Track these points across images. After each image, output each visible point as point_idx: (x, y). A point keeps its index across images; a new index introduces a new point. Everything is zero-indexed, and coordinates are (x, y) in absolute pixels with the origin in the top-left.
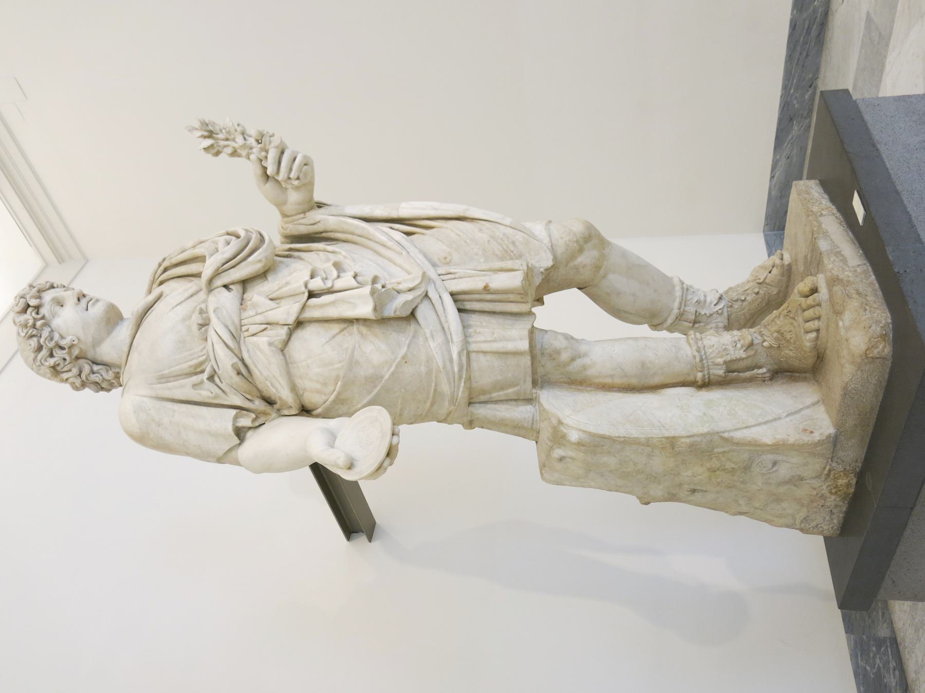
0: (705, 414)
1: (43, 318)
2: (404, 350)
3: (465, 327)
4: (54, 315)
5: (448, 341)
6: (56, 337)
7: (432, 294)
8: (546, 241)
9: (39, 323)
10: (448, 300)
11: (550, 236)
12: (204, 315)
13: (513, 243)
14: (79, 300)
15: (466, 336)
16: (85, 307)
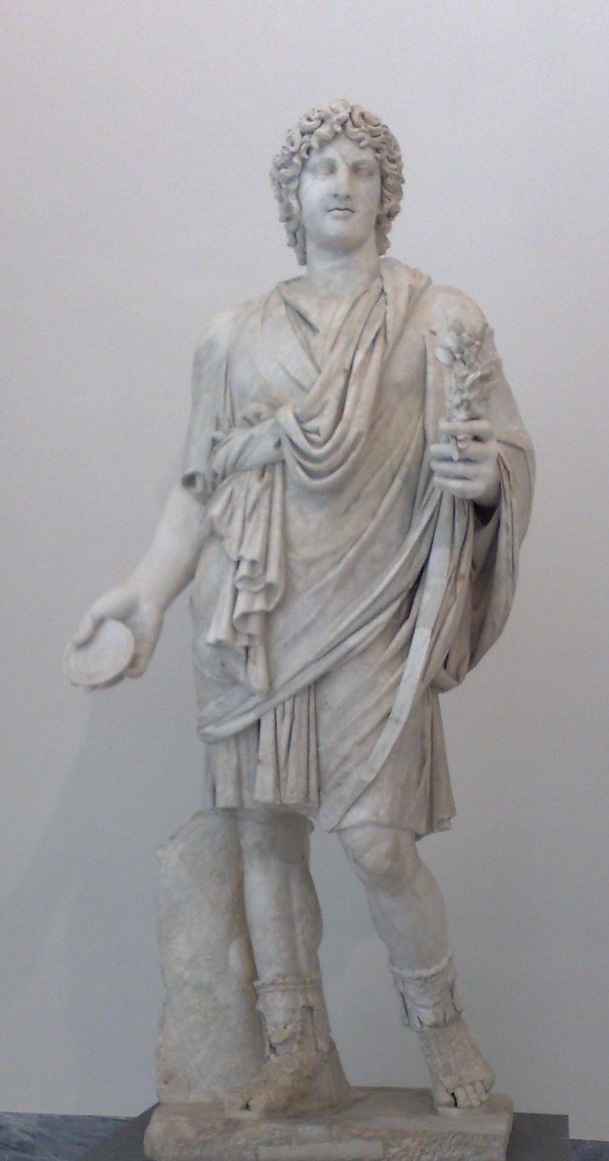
0: (185, 983)
1: (304, 161)
2: (208, 674)
3: (237, 736)
4: (314, 171)
5: (219, 721)
6: (293, 186)
7: (253, 701)
8: (346, 823)
9: (296, 160)
10: (251, 718)
11: (352, 827)
12: (255, 420)
13: (339, 785)
14: (336, 195)
15: (225, 740)
16: (331, 207)
